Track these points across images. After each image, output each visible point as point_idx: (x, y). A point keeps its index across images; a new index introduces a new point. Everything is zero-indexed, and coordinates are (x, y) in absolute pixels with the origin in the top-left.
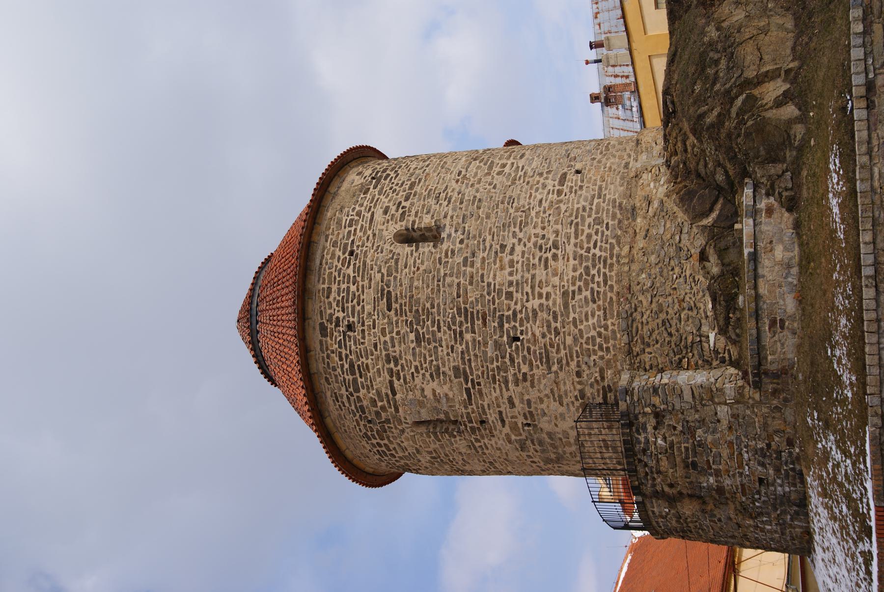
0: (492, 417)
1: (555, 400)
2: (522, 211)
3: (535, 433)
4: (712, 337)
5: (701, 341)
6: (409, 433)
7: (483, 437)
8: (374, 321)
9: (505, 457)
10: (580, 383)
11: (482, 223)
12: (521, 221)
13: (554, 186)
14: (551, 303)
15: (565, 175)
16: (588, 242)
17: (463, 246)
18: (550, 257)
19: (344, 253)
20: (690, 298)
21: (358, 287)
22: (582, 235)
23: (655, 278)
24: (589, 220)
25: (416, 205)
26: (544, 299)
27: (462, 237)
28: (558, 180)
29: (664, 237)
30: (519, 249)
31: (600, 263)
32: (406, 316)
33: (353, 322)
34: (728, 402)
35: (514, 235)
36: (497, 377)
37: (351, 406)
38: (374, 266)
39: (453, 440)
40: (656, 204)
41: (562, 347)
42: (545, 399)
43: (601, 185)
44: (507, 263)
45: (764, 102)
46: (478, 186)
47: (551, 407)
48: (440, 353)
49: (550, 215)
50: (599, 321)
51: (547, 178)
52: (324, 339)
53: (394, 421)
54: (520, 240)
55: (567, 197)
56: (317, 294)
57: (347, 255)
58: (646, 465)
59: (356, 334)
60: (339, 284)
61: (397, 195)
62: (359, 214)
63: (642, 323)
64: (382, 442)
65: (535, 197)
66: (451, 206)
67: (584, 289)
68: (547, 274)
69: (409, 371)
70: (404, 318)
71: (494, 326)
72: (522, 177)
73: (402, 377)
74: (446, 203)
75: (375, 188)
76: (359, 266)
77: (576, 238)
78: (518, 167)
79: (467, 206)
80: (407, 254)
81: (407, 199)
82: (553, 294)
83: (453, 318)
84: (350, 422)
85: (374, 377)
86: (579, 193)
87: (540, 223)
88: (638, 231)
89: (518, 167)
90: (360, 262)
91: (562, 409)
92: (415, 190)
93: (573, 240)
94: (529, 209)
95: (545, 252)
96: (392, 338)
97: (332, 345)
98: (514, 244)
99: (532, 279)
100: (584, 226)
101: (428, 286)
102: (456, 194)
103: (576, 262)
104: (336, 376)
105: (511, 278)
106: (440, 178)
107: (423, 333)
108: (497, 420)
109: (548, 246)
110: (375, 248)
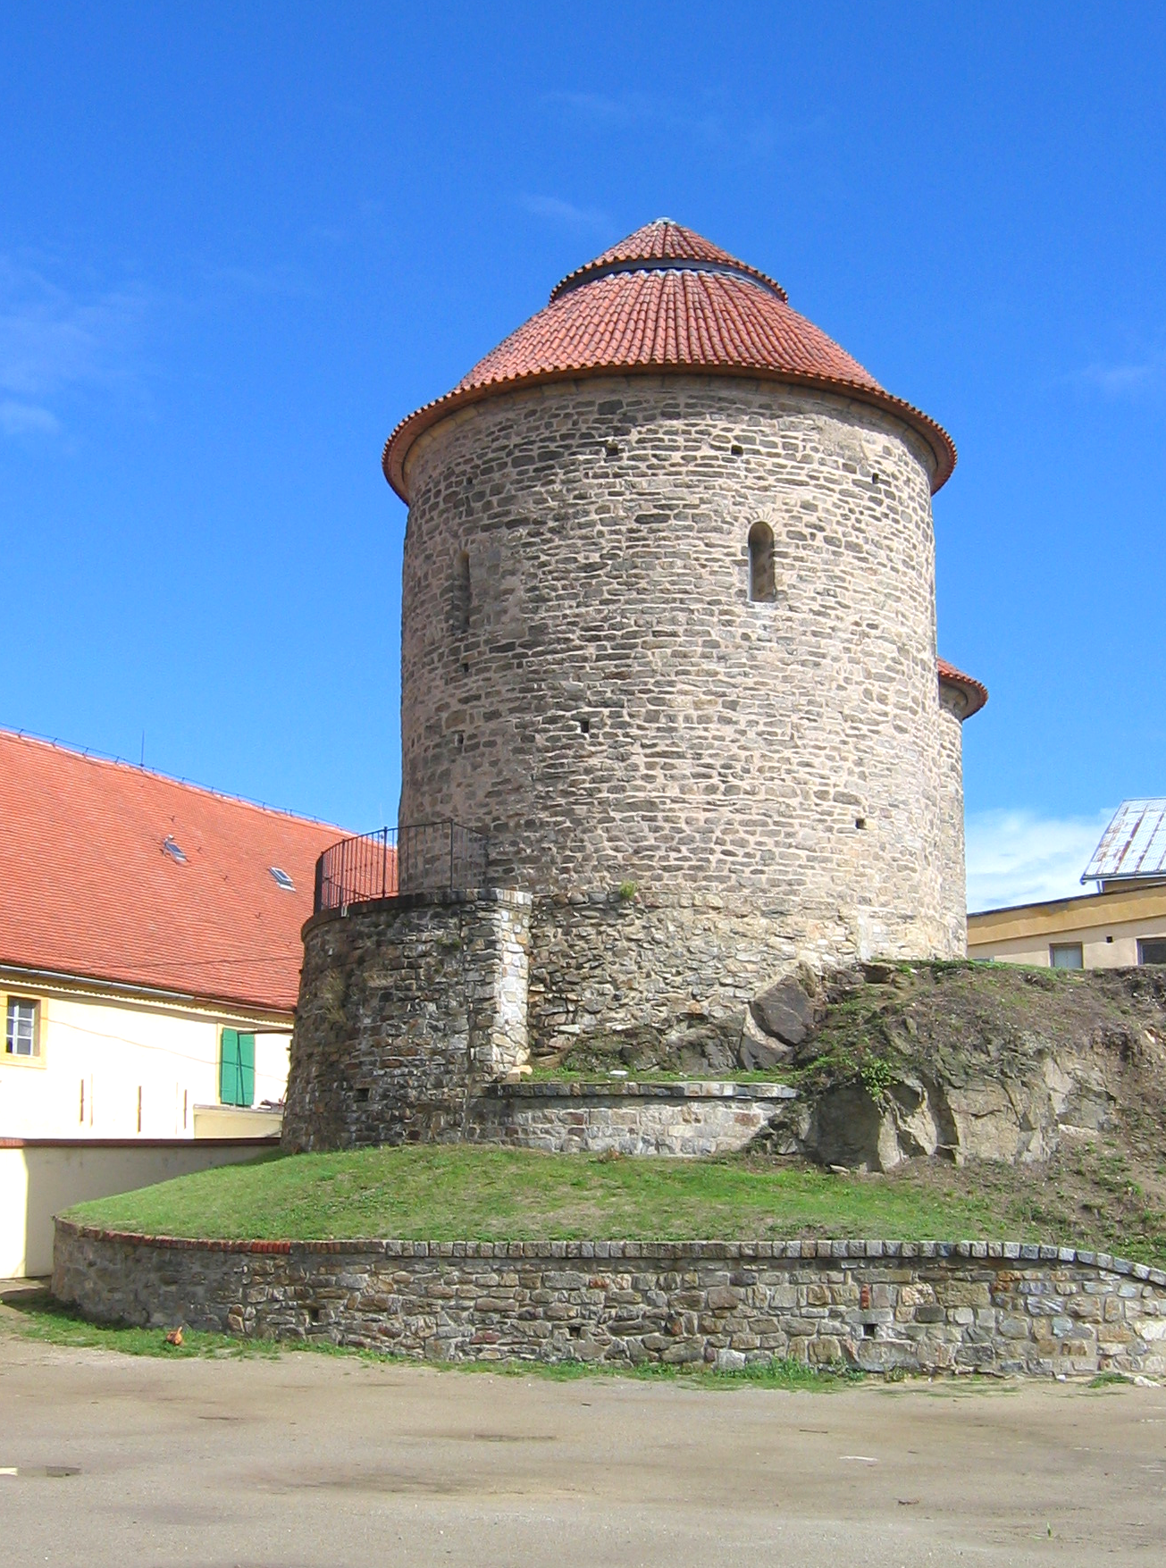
0: (473, 683)
1: (494, 784)
2: (792, 735)
3: (449, 751)
4: (575, 1029)
5: (568, 1012)
6: (452, 544)
7: (445, 666)
8: (620, 494)
9: (419, 699)
10: (518, 825)
11: (777, 669)
12: (775, 734)
13: (835, 785)
14: (639, 782)
15: (857, 802)
16: (733, 843)
17: (738, 640)
18: (711, 781)
19: (736, 438)
20: (633, 998)
21: (680, 465)
22: (746, 832)
23: (667, 947)
24: (770, 841)
25: (816, 558)
26: (646, 772)
27: (754, 637)
28: (846, 791)
29: (730, 960)
30: (728, 731)
31: (698, 861)
32: (628, 547)
33: (621, 459)
34: (472, 1050)
35: (751, 723)
36: (529, 695)
37: (493, 451)
38: (711, 492)
39: (442, 617)
40: (788, 948)
41: (572, 799)
42: (495, 770)
43: (831, 861)
44: (705, 712)
45: (909, 1119)
46: (846, 660)
47: (485, 779)
48: (567, 603)
49: (783, 780)
50: (609, 858)
51: (851, 773)
52: (596, 408)
53: (469, 522)
54: (743, 733)
55: (814, 808)
56: (669, 395)
57: (735, 443)
58: (389, 926)
59: (602, 463)
60: (684, 432)
61: (838, 523)
62: (806, 459)
63: (601, 925)
64: (441, 499)
65: (816, 756)
66: (811, 616)
67: (657, 835)
68: (684, 777)
69: (543, 551)
70: (624, 545)
71: (605, 692)
72: (856, 732)
73: (533, 540)
74: (816, 608)
75: (855, 482)
76: (712, 466)
77: (742, 823)
78: (877, 724)
79: (808, 644)
80: (729, 547)
81: (828, 540)
82: (652, 786)
83: (621, 626)
84: (469, 448)
85: (536, 493)
86: (820, 826)
87: (771, 764)
88: (745, 919)
89: (877, 724)
90: (719, 466)
91: (481, 794)
92: (846, 552)
93: (738, 817)
94: (797, 747)
95: (720, 774)
96: (591, 524)
97: (585, 421)
98: (736, 723)
99: (677, 753)
100: (761, 836)
101: (673, 583)
102: (832, 624)
103: (702, 823)
104: (537, 428)
105: (681, 719)
106: (865, 594)
107: (599, 576)
108: (468, 691)
109: (730, 778)
110: (743, 490)
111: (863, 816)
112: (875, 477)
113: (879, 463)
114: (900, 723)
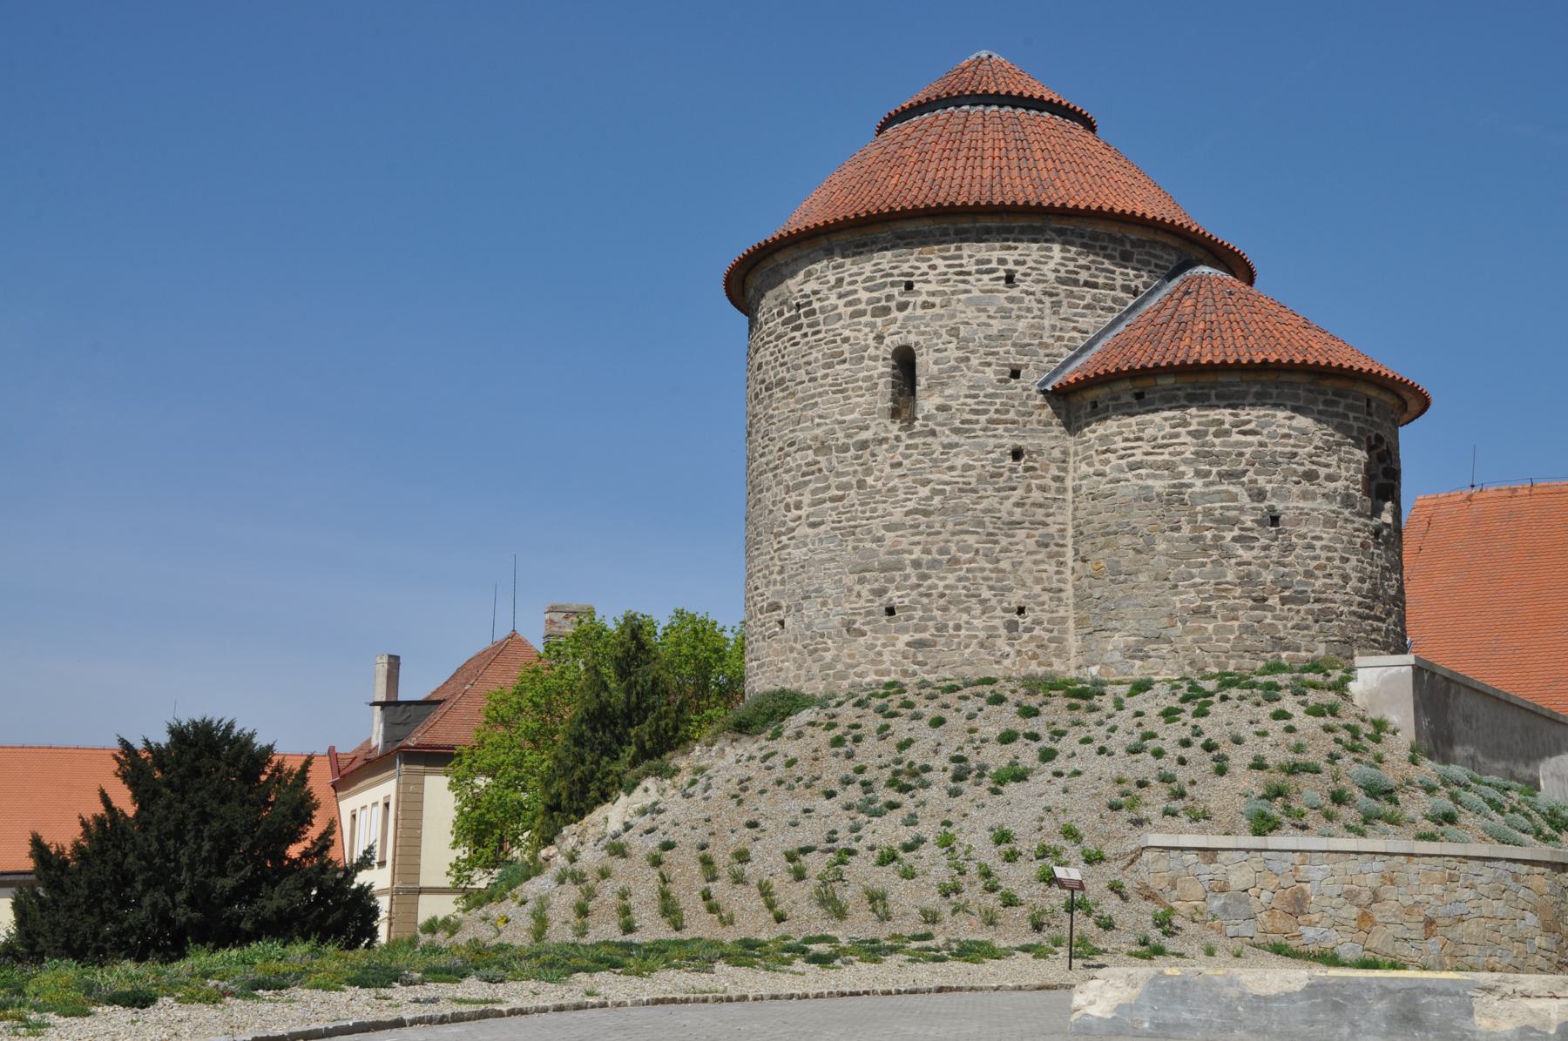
13: (768, 598)
75: (784, 324)
89: (793, 530)
111: (782, 618)
112: (798, 306)
113: (801, 290)
114: (811, 520)
